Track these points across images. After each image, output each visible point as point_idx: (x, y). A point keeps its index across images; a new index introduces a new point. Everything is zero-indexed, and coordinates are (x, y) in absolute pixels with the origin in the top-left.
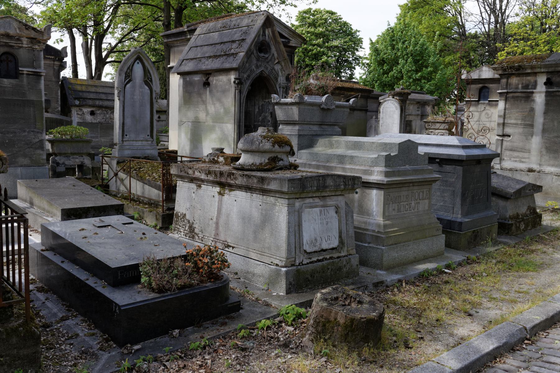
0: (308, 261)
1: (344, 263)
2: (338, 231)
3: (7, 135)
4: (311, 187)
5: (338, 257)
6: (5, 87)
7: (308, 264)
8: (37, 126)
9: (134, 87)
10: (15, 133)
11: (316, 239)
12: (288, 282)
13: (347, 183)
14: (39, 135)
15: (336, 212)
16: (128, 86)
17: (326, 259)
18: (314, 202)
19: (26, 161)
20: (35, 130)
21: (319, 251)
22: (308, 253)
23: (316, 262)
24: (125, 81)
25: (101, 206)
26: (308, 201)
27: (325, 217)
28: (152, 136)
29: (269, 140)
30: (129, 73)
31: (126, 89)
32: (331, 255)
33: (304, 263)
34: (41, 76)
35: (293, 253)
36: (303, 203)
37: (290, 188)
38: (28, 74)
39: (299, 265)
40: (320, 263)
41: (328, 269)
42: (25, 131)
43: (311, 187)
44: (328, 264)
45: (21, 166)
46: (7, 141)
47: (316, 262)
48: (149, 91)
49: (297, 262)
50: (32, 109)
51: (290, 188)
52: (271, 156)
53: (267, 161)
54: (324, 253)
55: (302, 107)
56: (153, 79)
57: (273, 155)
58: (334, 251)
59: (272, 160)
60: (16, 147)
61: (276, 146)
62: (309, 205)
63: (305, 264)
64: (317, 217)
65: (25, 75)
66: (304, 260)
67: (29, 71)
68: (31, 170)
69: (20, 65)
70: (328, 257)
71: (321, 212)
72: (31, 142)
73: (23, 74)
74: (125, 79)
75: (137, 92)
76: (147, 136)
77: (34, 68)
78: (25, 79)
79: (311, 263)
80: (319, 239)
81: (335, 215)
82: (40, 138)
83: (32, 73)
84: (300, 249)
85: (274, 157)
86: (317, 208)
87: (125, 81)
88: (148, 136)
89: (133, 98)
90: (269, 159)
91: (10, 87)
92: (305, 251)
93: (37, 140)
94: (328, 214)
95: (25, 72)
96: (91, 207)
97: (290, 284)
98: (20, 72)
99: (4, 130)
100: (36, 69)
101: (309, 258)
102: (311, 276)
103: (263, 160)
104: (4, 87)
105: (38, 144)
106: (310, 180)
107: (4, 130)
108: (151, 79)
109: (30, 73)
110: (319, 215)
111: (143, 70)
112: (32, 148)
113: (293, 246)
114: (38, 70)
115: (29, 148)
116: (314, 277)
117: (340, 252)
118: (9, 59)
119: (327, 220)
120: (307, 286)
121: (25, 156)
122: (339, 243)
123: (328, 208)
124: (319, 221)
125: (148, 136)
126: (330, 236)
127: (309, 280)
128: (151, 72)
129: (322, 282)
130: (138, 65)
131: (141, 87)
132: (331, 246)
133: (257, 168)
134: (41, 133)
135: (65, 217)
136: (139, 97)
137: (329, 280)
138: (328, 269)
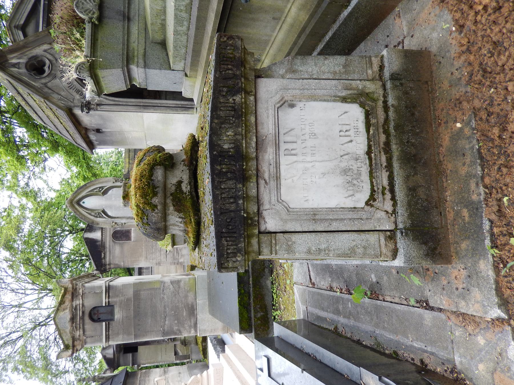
0: (388, 196)
6: (123, 316)
7: (393, 198)
8: (158, 287)
9: (110, 207)
10: (165, 306)
11: (345, 171)
14: (166, 285)
15: (292, 106)
16: (110, 213)
17: (387, 144)
21: (371, 165)
24: (104, 218)
27: (299, 142)
31: (114, 216)
40: (396, 165)
42: (163, 298)
46: (173, 312)
48: (114, 189)
50: (142, 292)
64: (301, 166)
71: (290, 153)
73: (109, 302)
74: (102, 217)
80: (343, 165)
81: (296, 110)
82: (169, 284)
83: (107, 294)
87: (104, 218)
91: (122, 312)
92: (367, 203)
93: (171, 286)
94: (293, 133)
95: (107, 300)
98: (107, 304)
100: (103, 290)
101: (383, 194)
104: (123, 318)
107: (163, 316)
109: (107, 296)
110: (294, 158)
115: (178, 293)
119: (307, 137)
121: (186, 297)
123: (282, 132)
124: (309, 158)
126: (339, 128)
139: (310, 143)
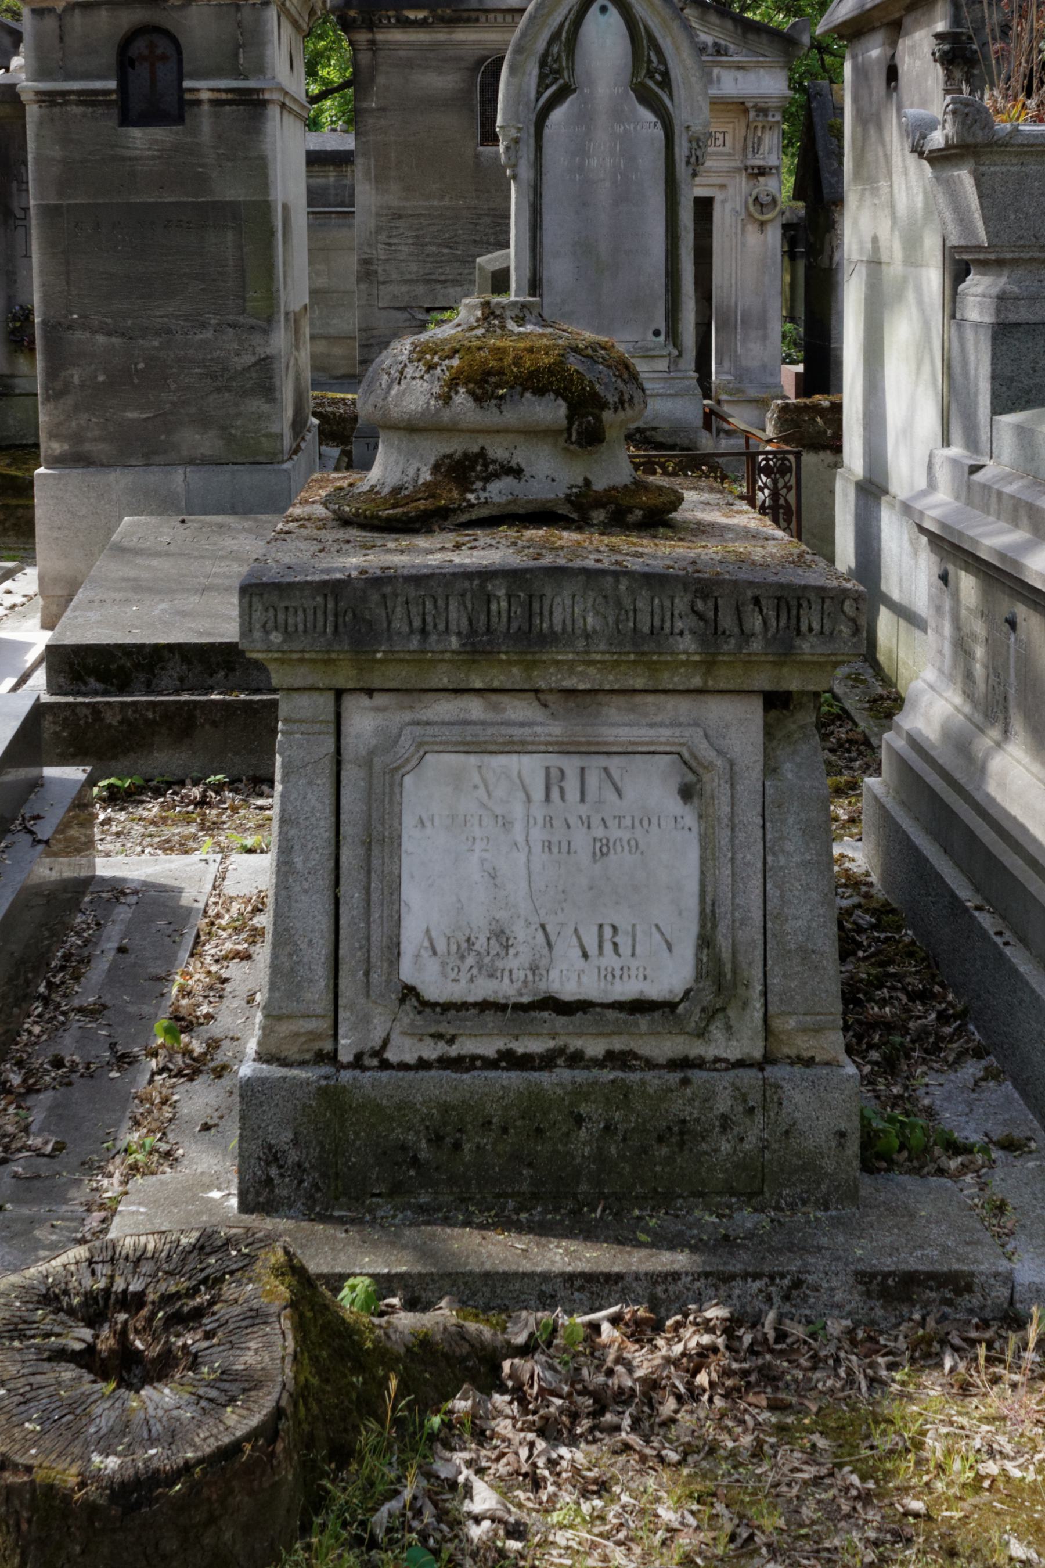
0: (431, 1051)
1: (723, 1104)
2: (692, 903)
3: (141, 342)
4: (424, 632)
5: (681, 1064)
6: (136, 159)
7: (423, 1064)
8: (249, 304)
9: (584, 118)
10: (169, 331)
11: (501, 936)
12: (255, 1148)
13: (727, 622)
14: (257, 339)
15: (686, 793)
16: (557, 115)
17: (576, 1059)
18: (490, 716)
19: (207, 443)
20: (241, 319)
21: (518, 1007)
22: (433, 1005)
23: (490, 1064)
24: (537, 99)
25: (212, 645)
26: (444, 708)
27: (584, 810)
28: (673, 334)
29: (431, 367)
30: (558, 59)
31: (547, 132)
32: (618, 1044)
33: (391, 1055)
34: (264, 104)
35: (317, 994)
36: (408, 716)
37: (257, 635)
38: (215, 103)
39: (358, 1064)
40: (513, 1079)
41: (579, 1120)
42: (203, 325)
43: (424, 632)
44: (580, 1093)
45: (191, 462)
46: (141, 366)
47: (490, 1064)
48: (659, 132)
49: (347, 1047)
50: (230, 236)
51: (257, 635)
52: (448, 451)
53: (426, 476)
54: (563, 1020)
55: (997, 168)
56: (676, 74)
57: (456, 446)
58: (643, 1022)
59: (451, 469)
60: (173, 386)
61: (461, 398)
62: (453, 734)
63: (404, 1066)
64: (518, 810)
65: (206, 107)
66: (396, 1039)
67: (219, 90)
68: (222, 477)
69: (187, 67)
70: (595, 1048)
71: (552, 781)
72: (224, 369)
73: (198, 103)
74: (541, 86)
75: (602, 137)
76: (650, 337)
77: (238, 74)
78: (205, 123)
79: (446, 1063)
80: (520, 933)
81: (674, 805)
82: (261, 352)
83: (230, 96)
84: (367, 974)
85: (466, 455)
86: (526, 759)
87: (539, 94)
88: (657, 333)
89: (581, 169)
90: (436, 468)
91: (153, 158)
92: (409, 992)
93: (249, 359)
94: (611, 795)
95: (205, 96)
96: (170, 647)
97: (273, 1156)
98: (188, 96)
99: (129, 322)
100: (246, 78)
101: (438, 1036)
102: (437, 1140)
103: (411, 472)
104: (130, 159)
105: (254, 375)
106: (412, 592)
107: (129, 322)
108: (666, 74)
109: (224, 96)
110: (538, 794)
111: (628, 41)
112: (228, 389)
113: (318, 953)
114: (251, 84)
115: (218, 390)
116: (457, 1146)
117: (702, 1034)
118: (159, 51)
119: (599, 832)
120: (396, 1190)
121: (204, 422)
122: (699, 976)
123: (614, 763)
124: (537, 834)
125: (657, 333)
126: (624, 926)
127: (415, 1161)
128: (666, 44)
129: (525, 1187)
130: (602, 19)
131: (618, 115)
132: (626, 990)
133: (357, 515)
134: (266, 332)
135: (62, 680)
136: (609, 162)
137: (584, 1187)
138: (579, 1120)
139: (581, 839)
